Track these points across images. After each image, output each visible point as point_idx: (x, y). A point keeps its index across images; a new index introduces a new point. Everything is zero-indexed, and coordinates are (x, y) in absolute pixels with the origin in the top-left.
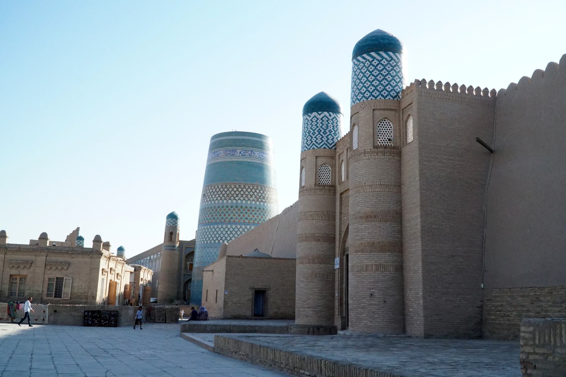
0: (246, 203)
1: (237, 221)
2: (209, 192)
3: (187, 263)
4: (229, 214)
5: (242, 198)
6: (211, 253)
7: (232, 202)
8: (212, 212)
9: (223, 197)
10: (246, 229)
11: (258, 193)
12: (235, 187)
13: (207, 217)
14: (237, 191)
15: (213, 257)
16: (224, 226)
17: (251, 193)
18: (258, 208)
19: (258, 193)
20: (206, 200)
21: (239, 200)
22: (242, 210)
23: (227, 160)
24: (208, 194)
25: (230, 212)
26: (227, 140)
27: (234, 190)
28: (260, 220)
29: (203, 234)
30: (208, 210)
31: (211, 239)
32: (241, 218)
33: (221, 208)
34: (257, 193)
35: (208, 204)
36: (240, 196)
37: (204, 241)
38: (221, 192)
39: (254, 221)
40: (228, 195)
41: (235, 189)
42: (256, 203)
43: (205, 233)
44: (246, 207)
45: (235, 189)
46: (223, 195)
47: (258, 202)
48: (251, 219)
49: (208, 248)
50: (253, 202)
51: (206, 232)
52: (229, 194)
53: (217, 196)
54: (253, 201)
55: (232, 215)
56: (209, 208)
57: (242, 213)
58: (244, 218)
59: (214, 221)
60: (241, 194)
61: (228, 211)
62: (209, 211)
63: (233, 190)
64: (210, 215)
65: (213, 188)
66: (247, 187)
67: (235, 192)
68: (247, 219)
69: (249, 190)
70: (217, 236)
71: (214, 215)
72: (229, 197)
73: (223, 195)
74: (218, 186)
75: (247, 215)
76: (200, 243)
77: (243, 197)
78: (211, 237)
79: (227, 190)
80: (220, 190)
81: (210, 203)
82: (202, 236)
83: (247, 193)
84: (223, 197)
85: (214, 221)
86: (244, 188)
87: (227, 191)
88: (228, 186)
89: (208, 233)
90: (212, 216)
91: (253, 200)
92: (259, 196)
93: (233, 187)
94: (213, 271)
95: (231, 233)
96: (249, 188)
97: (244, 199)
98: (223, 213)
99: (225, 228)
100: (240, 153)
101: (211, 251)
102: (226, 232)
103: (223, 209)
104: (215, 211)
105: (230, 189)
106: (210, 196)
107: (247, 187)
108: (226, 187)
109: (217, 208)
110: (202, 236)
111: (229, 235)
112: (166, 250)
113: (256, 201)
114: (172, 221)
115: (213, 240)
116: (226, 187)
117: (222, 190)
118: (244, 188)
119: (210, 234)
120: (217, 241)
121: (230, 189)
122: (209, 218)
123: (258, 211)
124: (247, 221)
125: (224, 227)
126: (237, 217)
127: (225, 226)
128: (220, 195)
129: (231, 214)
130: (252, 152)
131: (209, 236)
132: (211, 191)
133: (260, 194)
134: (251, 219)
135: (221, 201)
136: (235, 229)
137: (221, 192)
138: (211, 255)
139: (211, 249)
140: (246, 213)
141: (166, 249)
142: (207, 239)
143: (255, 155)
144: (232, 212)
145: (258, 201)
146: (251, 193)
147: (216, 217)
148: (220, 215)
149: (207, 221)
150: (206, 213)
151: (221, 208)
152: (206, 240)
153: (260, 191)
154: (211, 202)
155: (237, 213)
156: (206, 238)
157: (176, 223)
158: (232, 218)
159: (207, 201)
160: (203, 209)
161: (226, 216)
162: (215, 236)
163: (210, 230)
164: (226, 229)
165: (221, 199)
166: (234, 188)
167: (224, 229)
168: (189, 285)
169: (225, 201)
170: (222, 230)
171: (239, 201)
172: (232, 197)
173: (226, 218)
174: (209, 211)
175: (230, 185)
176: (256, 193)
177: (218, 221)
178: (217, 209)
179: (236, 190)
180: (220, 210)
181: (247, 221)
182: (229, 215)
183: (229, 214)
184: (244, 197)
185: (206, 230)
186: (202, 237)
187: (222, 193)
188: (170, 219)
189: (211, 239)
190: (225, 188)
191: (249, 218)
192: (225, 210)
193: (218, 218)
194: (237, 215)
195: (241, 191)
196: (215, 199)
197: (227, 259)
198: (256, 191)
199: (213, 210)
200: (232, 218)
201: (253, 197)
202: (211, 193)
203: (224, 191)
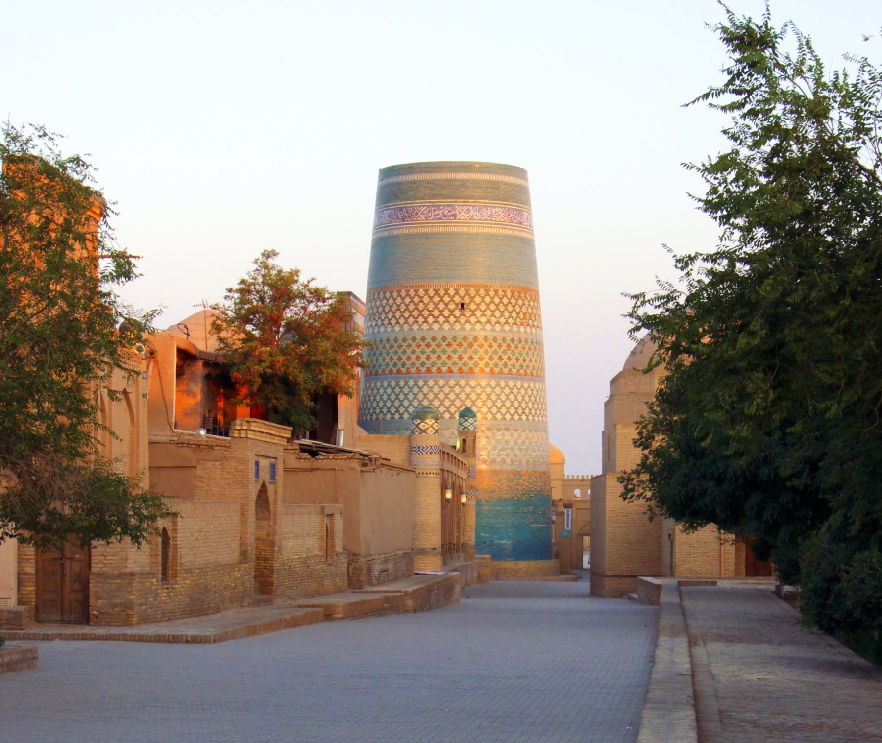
6: (507, 442)
15: (512, 451)
33: (516, 342)
49: (499, 430)
71: (505, 357)
90: (500, 358)
101: (508, 437)
120: (516, 417)
132: (487, 299)
138: (506, 446)
147: (509, 364)
149: (487, 370)
189: (503, 410)
196: (502, 320)
199: (500, 346)
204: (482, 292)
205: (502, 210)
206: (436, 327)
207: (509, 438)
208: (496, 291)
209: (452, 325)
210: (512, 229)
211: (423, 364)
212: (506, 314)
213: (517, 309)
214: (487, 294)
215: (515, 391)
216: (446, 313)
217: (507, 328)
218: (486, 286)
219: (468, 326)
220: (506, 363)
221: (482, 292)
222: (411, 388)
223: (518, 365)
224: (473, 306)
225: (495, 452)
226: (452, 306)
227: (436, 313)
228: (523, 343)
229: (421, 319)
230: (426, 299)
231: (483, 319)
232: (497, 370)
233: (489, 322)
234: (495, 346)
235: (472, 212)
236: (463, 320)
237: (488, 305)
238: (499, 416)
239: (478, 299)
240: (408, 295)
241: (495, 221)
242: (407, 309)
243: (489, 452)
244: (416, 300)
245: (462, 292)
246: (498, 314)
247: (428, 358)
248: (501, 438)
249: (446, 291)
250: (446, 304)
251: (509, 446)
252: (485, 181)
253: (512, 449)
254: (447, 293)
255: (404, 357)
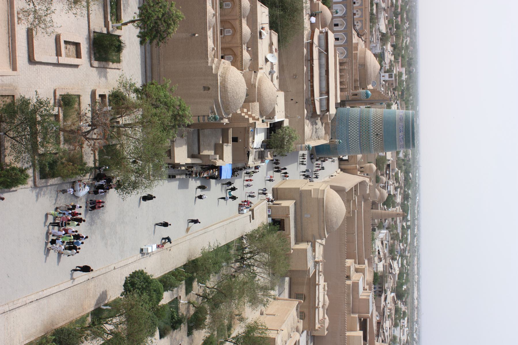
6: (344, 147)
64: (364, 143)
90: (365, 144)
101: (345, 147)
120: (350, 149)
132: (379, 141)
147: (364, 146)
174: (367, 142)
196: (374, 145)
199: (368, 144)
204: (381, 139)
206: (372, 128)
208: (382, 143)
209: (372, 132)
211: (362, 125)
212: (376, 145)
213: (378, 148)
214: (381, 141)
215: (357, 148)
216: (375, 131)
217: (373, 146)
219: (372, 136)
221: (381, 139)
222: (356, 122)
224: (377, 137)
226: (377, 132)
227: (375, 128)
229: (374, 124)
230: (379, 126)
231: (374, 140)
233: (374, 141)
234: (368, 143)
235: (401, 136)
236: (374, 135)
237: (378, 141)
238: (350, 144)
239: (379, 138)
240: (380, 121)
242: (377, 121)
244: (379, 123)
245: (381, 135)
246: (376, 143)
247: (364, 127)
249: (381, 131)
250: (378, 131)
252: (410, 139)
254: (380, 131)
255: (364, 120)
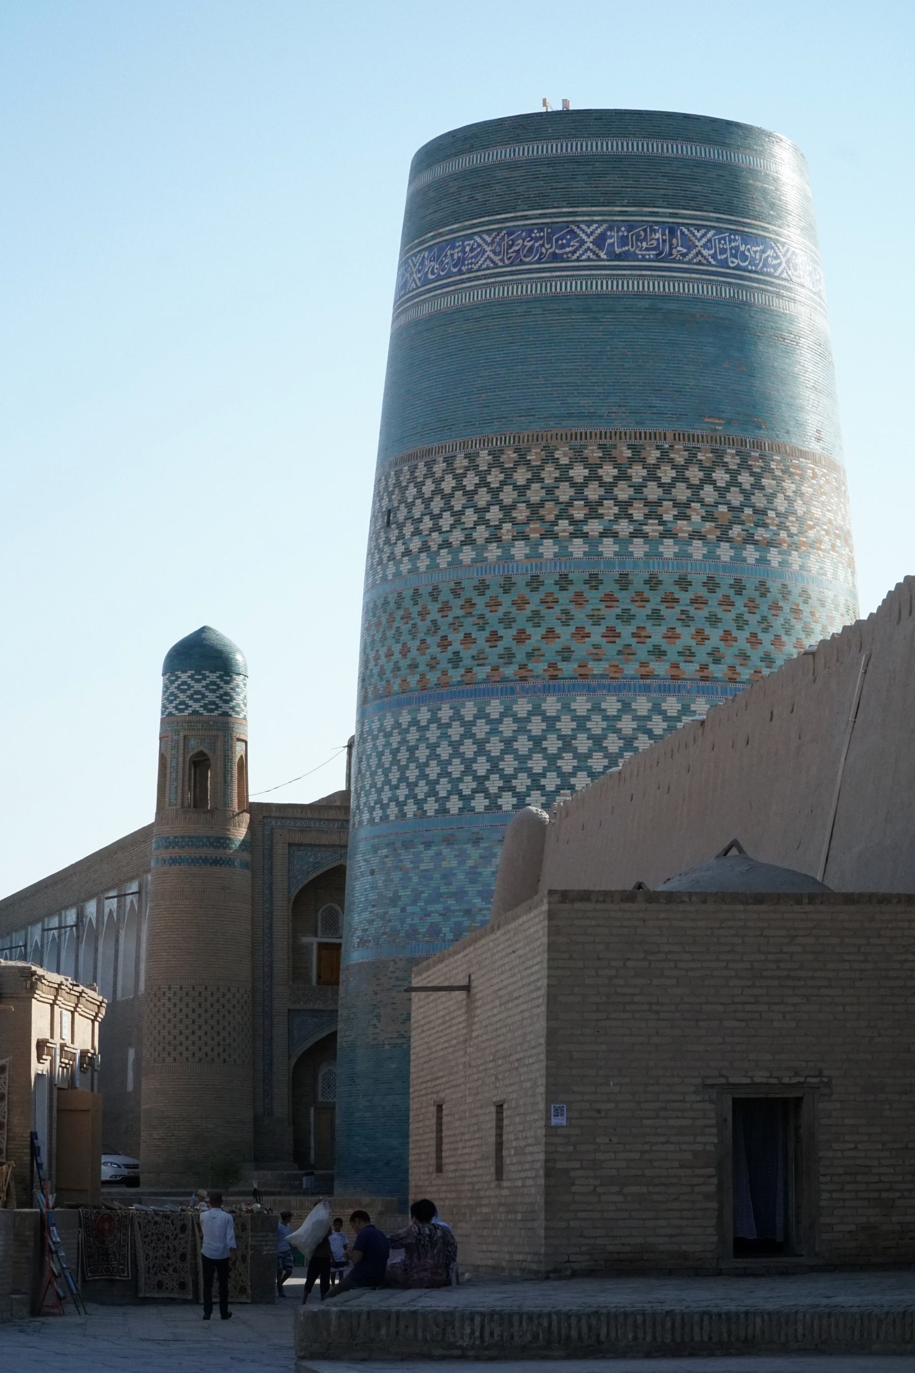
0: (654, 554)
1: (597, 668)
2: (420, 494)
3: (306, 940)
4: (551, 631)
5: (624, 528)
6: (447, 876)
7: (563, 554)
8: (440, 621)
9: (507, 526)
10: (657, 718)
11: (722, 492)
12: (579, 457)
13: (414, 653)
14: (594, 485)
16: (522, 707)
17: (681, 492)
18: (726, 580)
19: (722, 492)
20: (400, 549)
21: (608, 541)
22: (624, 598)
23: (516, 291)
24: (410, 506)
25: (551, 617)
26: (511, 166)
27: (570, 479)
28: (744, 657)
29: (395, 761)
30: (415, 610)
31: (443, 788)
32: (627, 652)
33: (494, 590)
34: (717, 488)
35: (414, 570)
36: (610, 509)
37: (401, 805)
38: (495, 493)
39: (704, 667)
40: (535, 509)
41: (579, 472)
42: (711, 555)
43: (403, 755)
44: (653, 582)
45: (579, 472)
46: (507, 510)
47: (725, 545)
48: (688, 654)
49: (428, 845)
50: (698, 550)
51: (412, 750)
52: (541, 504)
53: (470, 517)
54: (697, 543)
55: (565, 633)
56: (425, 599)
57: (626, 617)
58: (642, 652)
59: (456, 675)
60: (617, 503)
61: (544, 611)
62: (423, 614)
63: (564, 477)
64: (433, 641)
65: (439, 468)
66: (653, 456)
67: (579, 488)
68: (658, 653)
69: (667, 474)
70: (481, 767)
71: (456, 638)
72: (542, 519)
73: (507, 510)
74: (472, 458)
75: (663, 629)
76: (378, 813)
77: (630, 517)
78: (445, 773)
79: (530, 481)
80: (484, 483)
81: (424, 562)
82: (386, 773)
83: (653, 492)
84: (507, 526)
85: (456, 675)
86: (632, 461)
87: (527, 487)
88: (533, 457)
89: (422, 753)
90: (444, 643)
91: (697, 535)
92: (731, 509)
93: (564, 461)
94: (467, 988)
95: (567, 744)
96: (664, 457)
97: (637, 533)
98: (508, 621)
99: (527, 720)
100: (600, 241)
102: (537, 741)
103: (506, 600)
104: (460, 613)
105: (550, 474)
106: (427, 523)
107: (653, 456)
108: (522, 460)
109: (469, 592)
110: (386, 773)
111: (552, 760)
112: (176, 868)
113: (712, 537)
114: (198, 686)
115: (454, 798)
116: (522, 460)
117: (495, 478)
118: (632, 461)
119: (433, 755)
121: (550, 474)
122: (423, 660)
123: (727, 602)
124: (660, 668)
125: (522, 714)
126: (596, 646)
127: (529, 707)
128: (486, 509)
129: (559, 629)
130: (672, 232)
131: (433, 771)
133: (735, 497)
134: (688, 654)
135: (493, 552)
136: (588, 718)
137: (495, 493)
138: (443, 889)
139: (446, 851)
140: (656, 616)
141: (174, 861)
142: (422, 790)
143: (689, 250)
144: (566, 612)
145: (724, 537)
146: (681, 492)
147: (467, 655)
148: (494, 638)
149: (413, 680)
150: (405, 628)
151: (494, 590)
152: (412, 795)
153: (734, 474)
154: (433, 556)
155: (596, 619)
156: (412, 786)
157: (227, 698)
158: (566, 654)
159: (407, 553)
160: (386, 602)
161: (528, 646)
162: (468, 770)
163: (433, 734)
164: (537, 726)
165: (495, 538)
166: (569, 467)
167: (522, 723)
168: (323, 1071)
169: (520, 550)
170: (508, 734)
171: (609, 548)
172: (564, 524)
173: (530, 655)
174: (423, 614)
175: (545, 448)
176: (708, 488)
177: (481, 673)
178: (470, 603)
179: (587, 479)
180: (494, 604)
181: (660, 668)
182: (551, 634)
183: (551, 631)
184: (638, 515)
185: (413, 736)
186: (387, 782)
187: (495, 500)
188: (184, 677)
189: (443, 788)
190: (517, 464)
191: (672, 650)
192: (521, 603)
193: (479, 658)
194: (597, 634)
195: (617, 478)
196: (457, 536)
197: (551, 915)
198: (708, 480)
199: (445, 608)
200: (566, 654)
201: (696, 518)
202: (427, 502)
203: (508, 489)
205: (489, 239)
207: (454, 863)
210: (518, 282)
218: (429, 451)
220: (456, 653)
223: (493, 655)
225: (416, 909)
228: (521, 589)
232: (433, 677)
241: (470, 271)
243: (403, 910)
248: (431, 866)
251: (452, 889)
253: (460, 895)
